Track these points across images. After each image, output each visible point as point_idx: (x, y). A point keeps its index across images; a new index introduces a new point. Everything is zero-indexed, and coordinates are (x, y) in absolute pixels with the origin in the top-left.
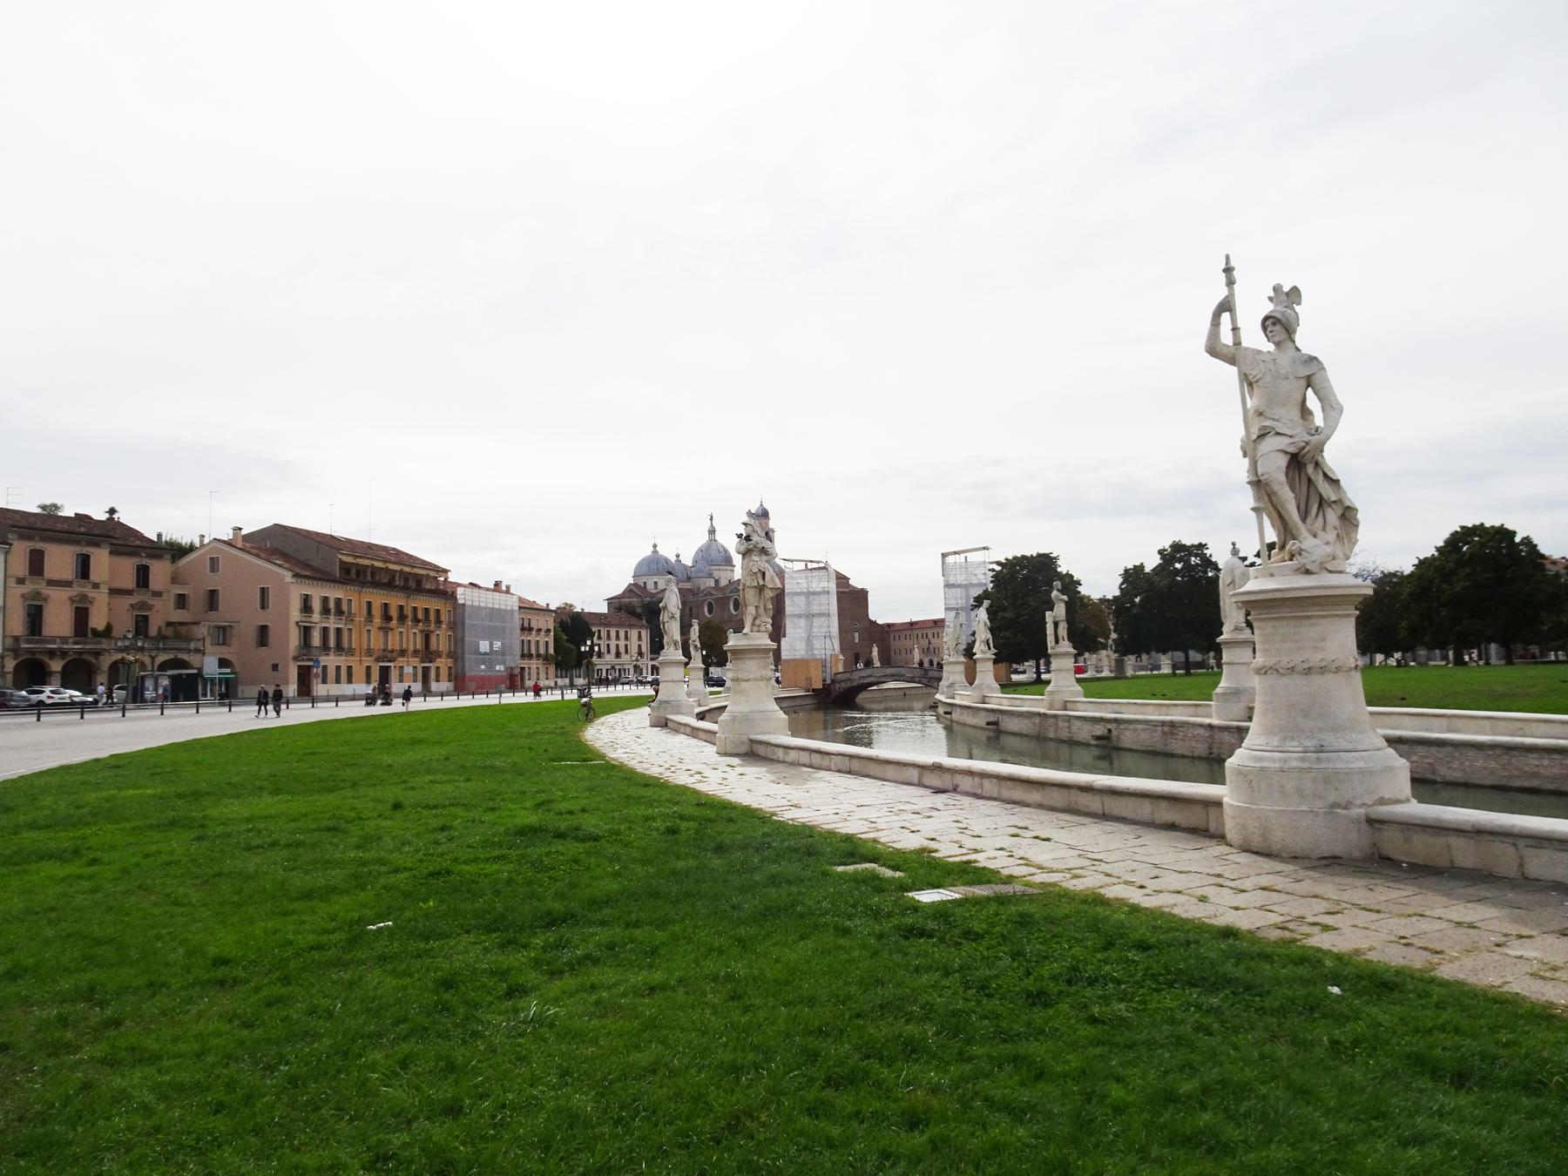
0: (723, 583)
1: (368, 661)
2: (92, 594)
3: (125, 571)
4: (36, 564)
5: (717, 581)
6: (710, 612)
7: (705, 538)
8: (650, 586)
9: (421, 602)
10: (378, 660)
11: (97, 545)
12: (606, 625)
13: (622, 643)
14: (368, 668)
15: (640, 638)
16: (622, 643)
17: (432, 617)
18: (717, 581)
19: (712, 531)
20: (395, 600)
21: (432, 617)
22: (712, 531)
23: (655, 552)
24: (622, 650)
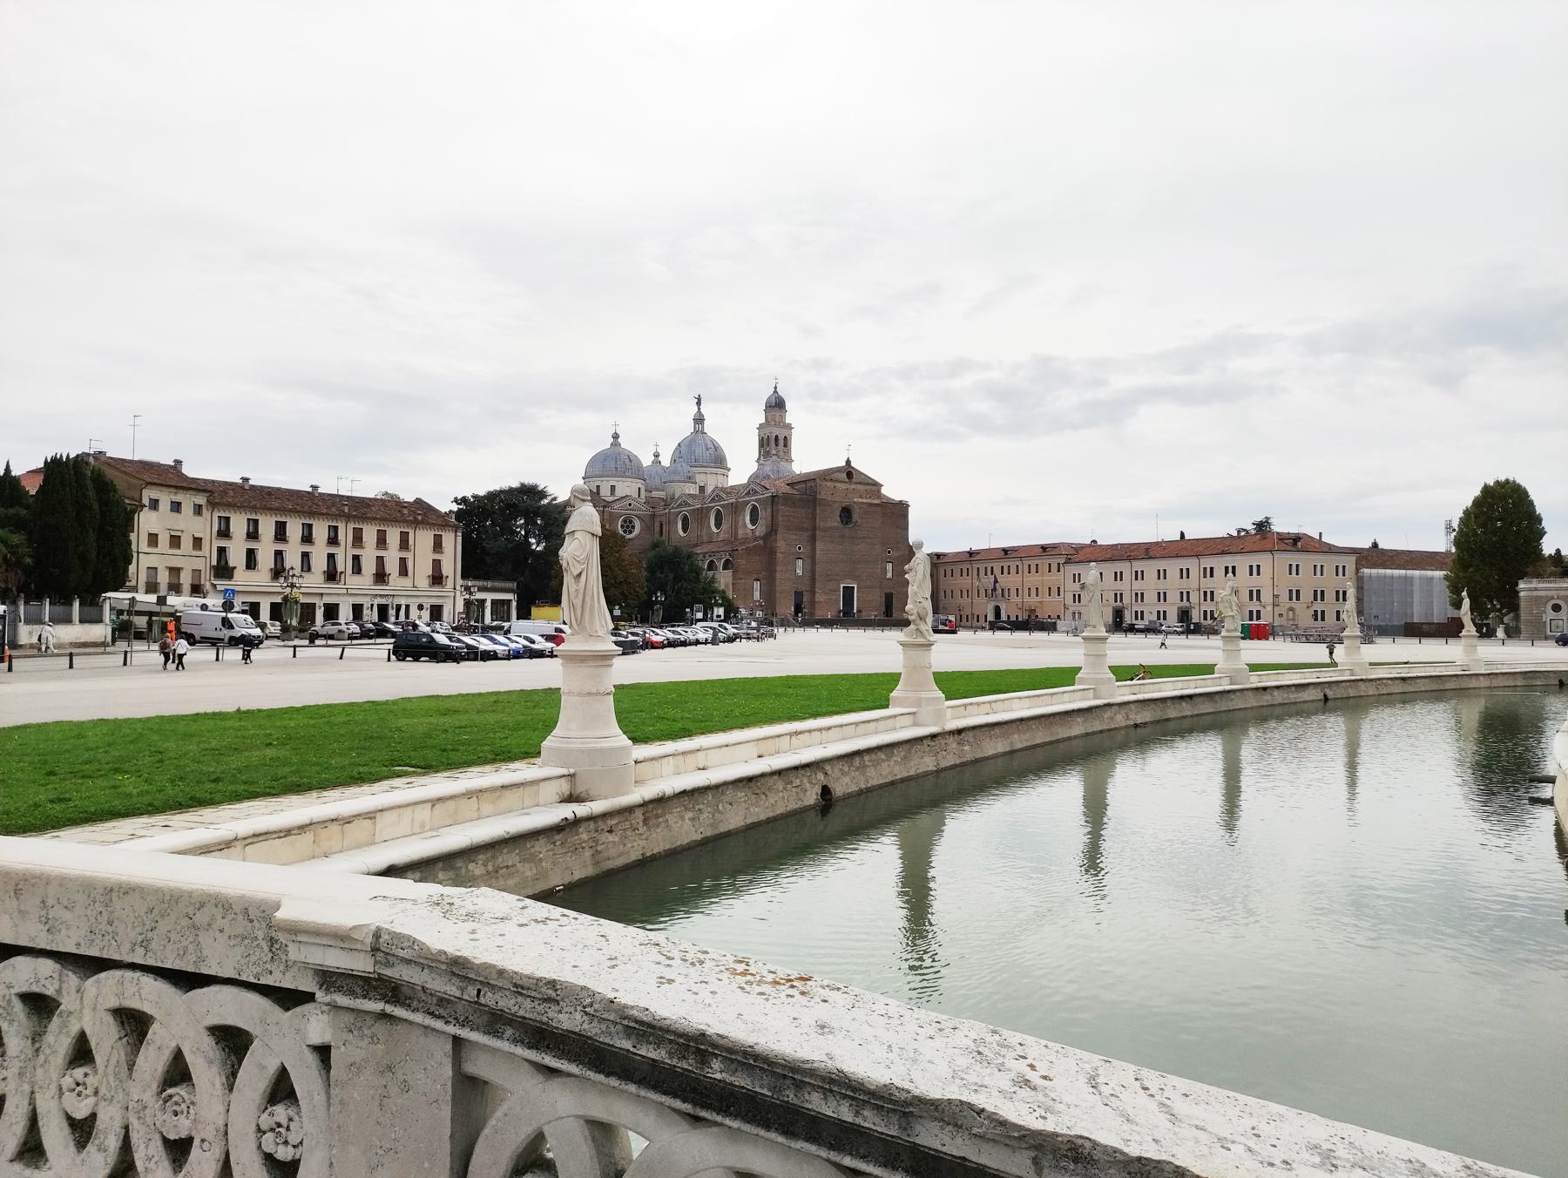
0: (709, 490)
5: (702, 489)
6: (685, 530)
7: (688, 428)
12: (348, 518)
13: (392, 556)
15: (438, 545)
16: (392, 556)
18: (702, 489)
19: (699, 420)
22: (699, 420)
24: (392, 567)
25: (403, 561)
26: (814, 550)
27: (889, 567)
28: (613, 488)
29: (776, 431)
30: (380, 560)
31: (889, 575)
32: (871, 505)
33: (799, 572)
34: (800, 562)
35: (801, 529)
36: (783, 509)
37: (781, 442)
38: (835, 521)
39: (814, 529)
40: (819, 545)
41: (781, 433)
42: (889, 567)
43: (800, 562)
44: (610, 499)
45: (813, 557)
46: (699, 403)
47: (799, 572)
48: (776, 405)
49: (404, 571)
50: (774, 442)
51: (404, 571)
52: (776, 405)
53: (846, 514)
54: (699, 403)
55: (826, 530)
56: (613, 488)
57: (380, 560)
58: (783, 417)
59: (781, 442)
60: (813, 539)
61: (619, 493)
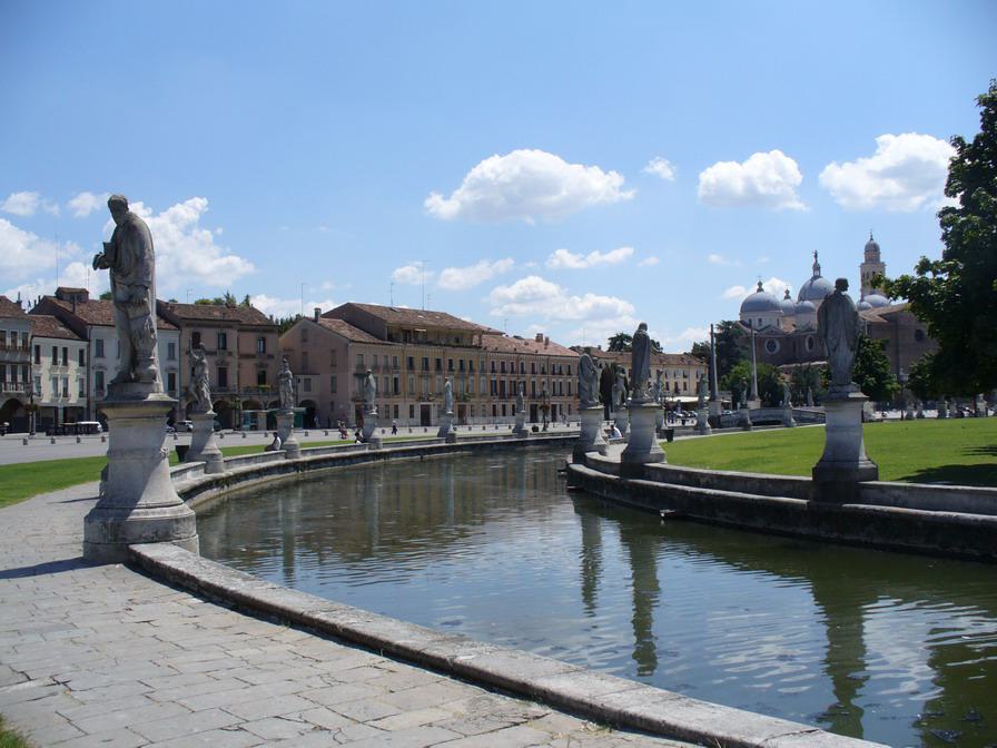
1: (411, 401)
2: (228, 359)
3: (249, 343)
4: (196, 338)
6: (811, 347)
7: (811, 274)
8: (755, 323)
9: (457, 355)
10: (420, 399)
11: (231, 327)
14: (412, 407)
16: (681, 381)
17: (467, 366)
19: (817, 267)
20: (433, 353)
21: (467, 366)
22: (817, 267)
23: (760, 290)
24: (681, 387)
25: (685, 384)
26: (898, 359)
28: (760, 320)
30: (676, 384)
40: (901, 356)
44: (759, 328)
46: (816, 256)
49: (685, 389)
51: (685, 389)
54: (816, 256)
56: (760, 320)
57: (676, 384)
58: (878, 258)
61: (764, 324)
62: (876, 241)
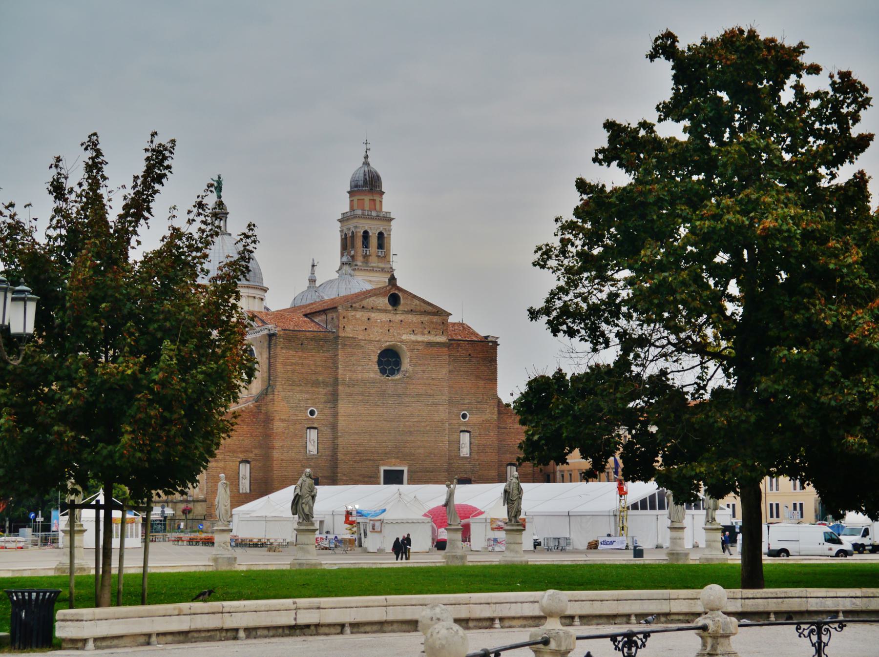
26: (335, 415)
27: (465, 438)
29: (364, 225)
31: (465, 451)
32: (430, 344)
33: (312, 449)
34: (313, 435)
35: (316, 384)
36: (283, 354)
37: (374, 241)
38: (372, 371)
39: (336, 382)
41: (374, 229)
42: (465, 438)
43: (313, 435)
45: (334, 427)
47: (312, 449)
48: (368, 185)
50: (364, 242)
52: (368, 185)
53: (389, 360)
55: (353, 384)
59: (374, 241)
60: (334, 398)
62: (376, 165)
